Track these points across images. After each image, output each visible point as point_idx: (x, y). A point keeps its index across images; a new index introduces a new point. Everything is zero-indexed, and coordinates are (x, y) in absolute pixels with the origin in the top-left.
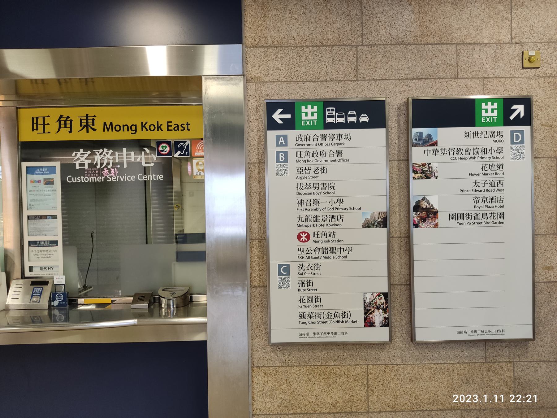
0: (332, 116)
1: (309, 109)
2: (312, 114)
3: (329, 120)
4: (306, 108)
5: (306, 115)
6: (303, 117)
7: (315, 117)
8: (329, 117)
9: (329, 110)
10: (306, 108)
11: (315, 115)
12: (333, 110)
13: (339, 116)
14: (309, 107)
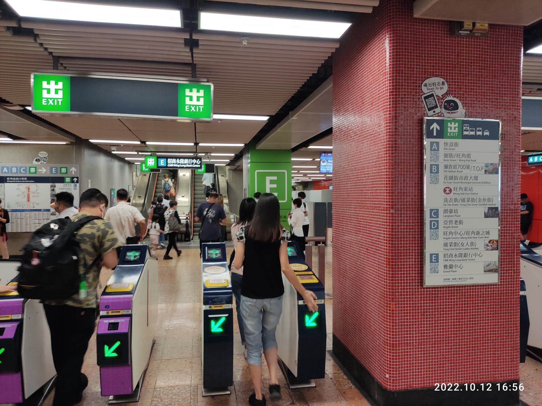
0: (467, 131)
1: (453, 125)
2: (455, 129)
3: (465, 133)
4: (451, 124)
5: (451, 129)
6: (449, 130)
7: (457, 130)
8: (466, 130)
9: (465, 126)
10: (451, 124)
11: (457, 129)
12: (467, 126)
13: (472, 131)
14: (453, 123)
